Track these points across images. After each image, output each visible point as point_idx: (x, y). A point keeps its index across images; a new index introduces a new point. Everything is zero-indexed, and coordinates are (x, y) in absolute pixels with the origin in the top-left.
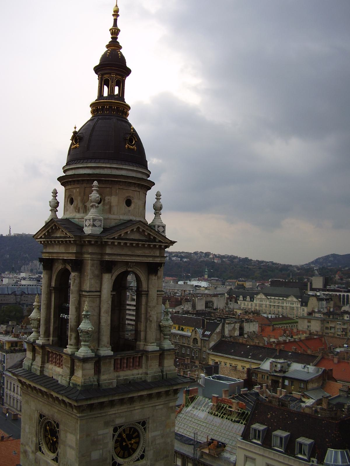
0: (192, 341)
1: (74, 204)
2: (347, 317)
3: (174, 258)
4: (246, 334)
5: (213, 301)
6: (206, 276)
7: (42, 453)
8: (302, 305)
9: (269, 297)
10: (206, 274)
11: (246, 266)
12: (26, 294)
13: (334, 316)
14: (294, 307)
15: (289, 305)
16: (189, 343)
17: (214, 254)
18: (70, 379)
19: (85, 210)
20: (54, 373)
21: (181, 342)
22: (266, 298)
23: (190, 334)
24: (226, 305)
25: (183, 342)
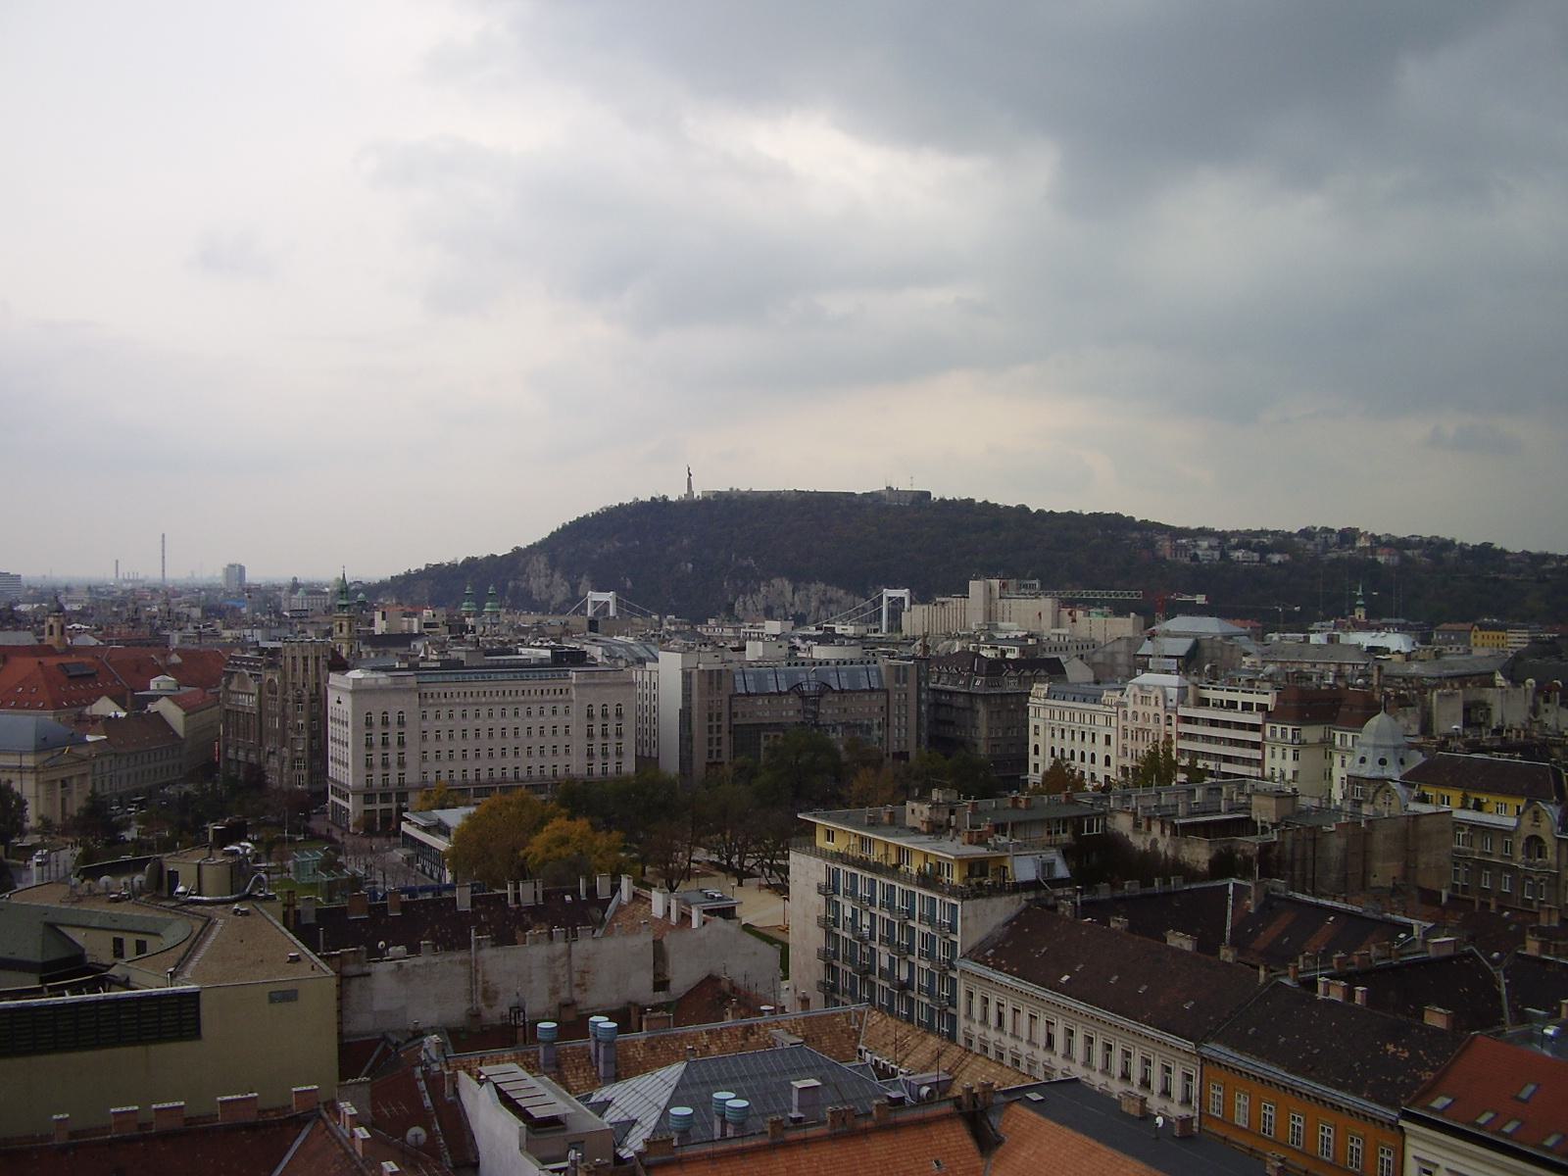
0: (1520, 845)
3: (1238, 554)
5: (1489, 702)
6: (1360, 614)
10: (1361, 606)
11: (1492, 574)
12: (834, 691)
16: (1508, 854)
17: (1373, 536)
21: (1477, 851)
23: (1511, 822)
24: (1532, 717)
25: (1484, 849)
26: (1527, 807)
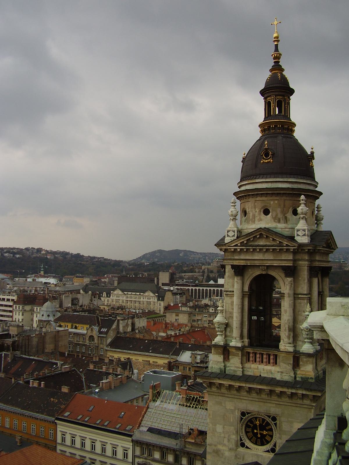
0: (87, 338)
1: (272, 215)
2: (212, 310)
3: (6, 255)
4: (137, 329)
5: (78, 298)
6: (42, 273)
7: (247, 447)
8: (158, 300)
9: (126, 293)
10: (42, 270)
11: (80, 262)
13: (200, 309)
14: (150, 302)
15: (146, 300)
16: (84, 341)
17: (46, 250)
18: (295, 374)
19: (285, 221)
20: (262, 371)
21: (75, 340)
22: (122, 293)
23: (85, 332)
24: (90, 302)
25: (78, 340)
26: (89, 328)
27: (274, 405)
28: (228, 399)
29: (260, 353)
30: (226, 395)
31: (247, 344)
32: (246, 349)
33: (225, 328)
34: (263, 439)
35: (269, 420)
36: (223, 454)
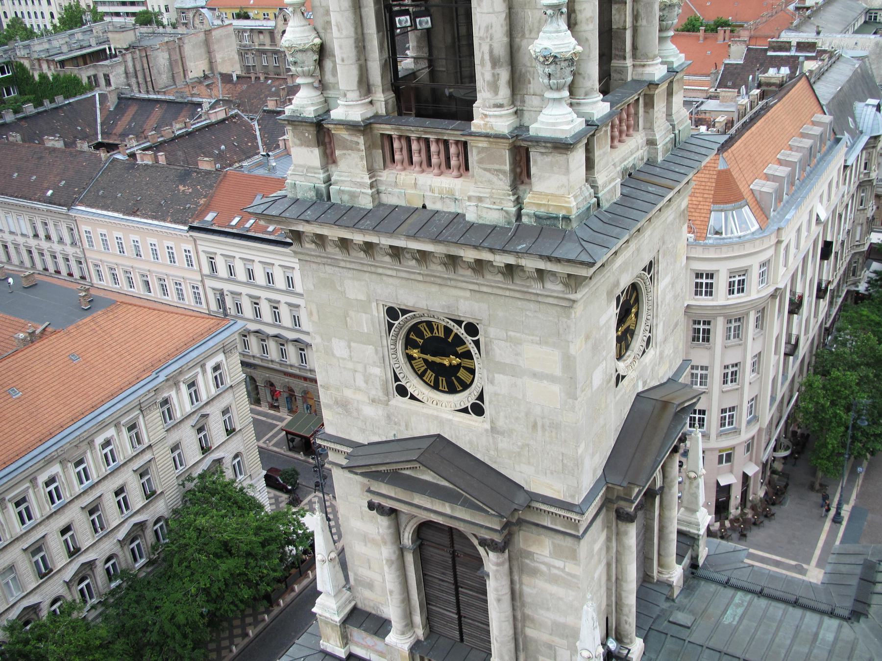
7: (413, 397)
18: (518, 202)
20: (428, 194)
26: (279, 14)
27: (468, 294)
28: (350, 274)
29: (419, 139)
30: (342, 264)
31: (382, 111)
32: (378, 126)
33: (320, 63)
34: (453, 378)
35: (461, 331)
36: (358, 410)
